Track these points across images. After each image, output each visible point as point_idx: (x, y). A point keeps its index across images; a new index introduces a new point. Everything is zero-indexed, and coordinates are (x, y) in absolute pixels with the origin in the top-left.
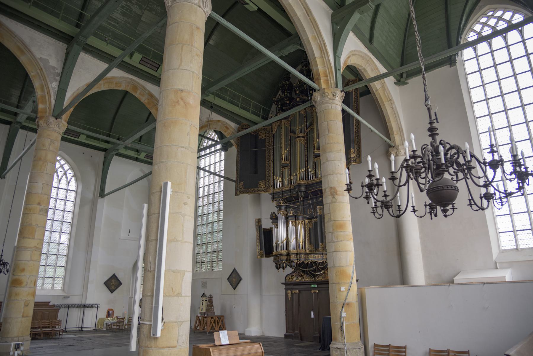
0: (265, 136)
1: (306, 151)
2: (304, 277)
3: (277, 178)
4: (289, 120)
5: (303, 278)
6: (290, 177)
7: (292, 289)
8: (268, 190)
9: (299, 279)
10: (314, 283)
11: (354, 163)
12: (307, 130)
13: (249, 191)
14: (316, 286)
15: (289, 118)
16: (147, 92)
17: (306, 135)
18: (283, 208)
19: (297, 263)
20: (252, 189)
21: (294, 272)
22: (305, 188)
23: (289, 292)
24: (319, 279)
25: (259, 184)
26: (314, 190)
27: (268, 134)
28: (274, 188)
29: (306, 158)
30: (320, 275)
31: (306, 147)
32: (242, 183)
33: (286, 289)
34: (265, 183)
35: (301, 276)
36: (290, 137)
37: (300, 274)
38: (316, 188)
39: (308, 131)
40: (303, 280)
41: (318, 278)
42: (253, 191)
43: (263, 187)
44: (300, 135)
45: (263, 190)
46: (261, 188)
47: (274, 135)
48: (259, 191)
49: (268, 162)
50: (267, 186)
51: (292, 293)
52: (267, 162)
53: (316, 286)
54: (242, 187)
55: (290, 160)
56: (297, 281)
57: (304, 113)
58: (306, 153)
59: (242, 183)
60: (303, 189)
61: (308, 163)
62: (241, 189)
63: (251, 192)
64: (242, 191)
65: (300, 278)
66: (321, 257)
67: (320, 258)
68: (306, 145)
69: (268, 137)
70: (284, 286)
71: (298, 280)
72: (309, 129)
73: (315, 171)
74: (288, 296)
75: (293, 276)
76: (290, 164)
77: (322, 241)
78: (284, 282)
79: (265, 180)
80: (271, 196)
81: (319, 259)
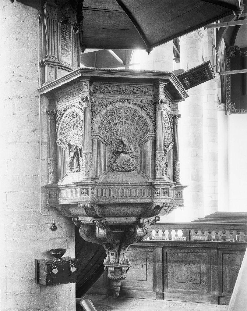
13: (240, 111)
20: (243, 109)
32: (234, 103)
42: (244, 111)
54: (234, 107)
59: (234, 103)
62: (233, 109)
63: (242, 112)
64: (234, 111)
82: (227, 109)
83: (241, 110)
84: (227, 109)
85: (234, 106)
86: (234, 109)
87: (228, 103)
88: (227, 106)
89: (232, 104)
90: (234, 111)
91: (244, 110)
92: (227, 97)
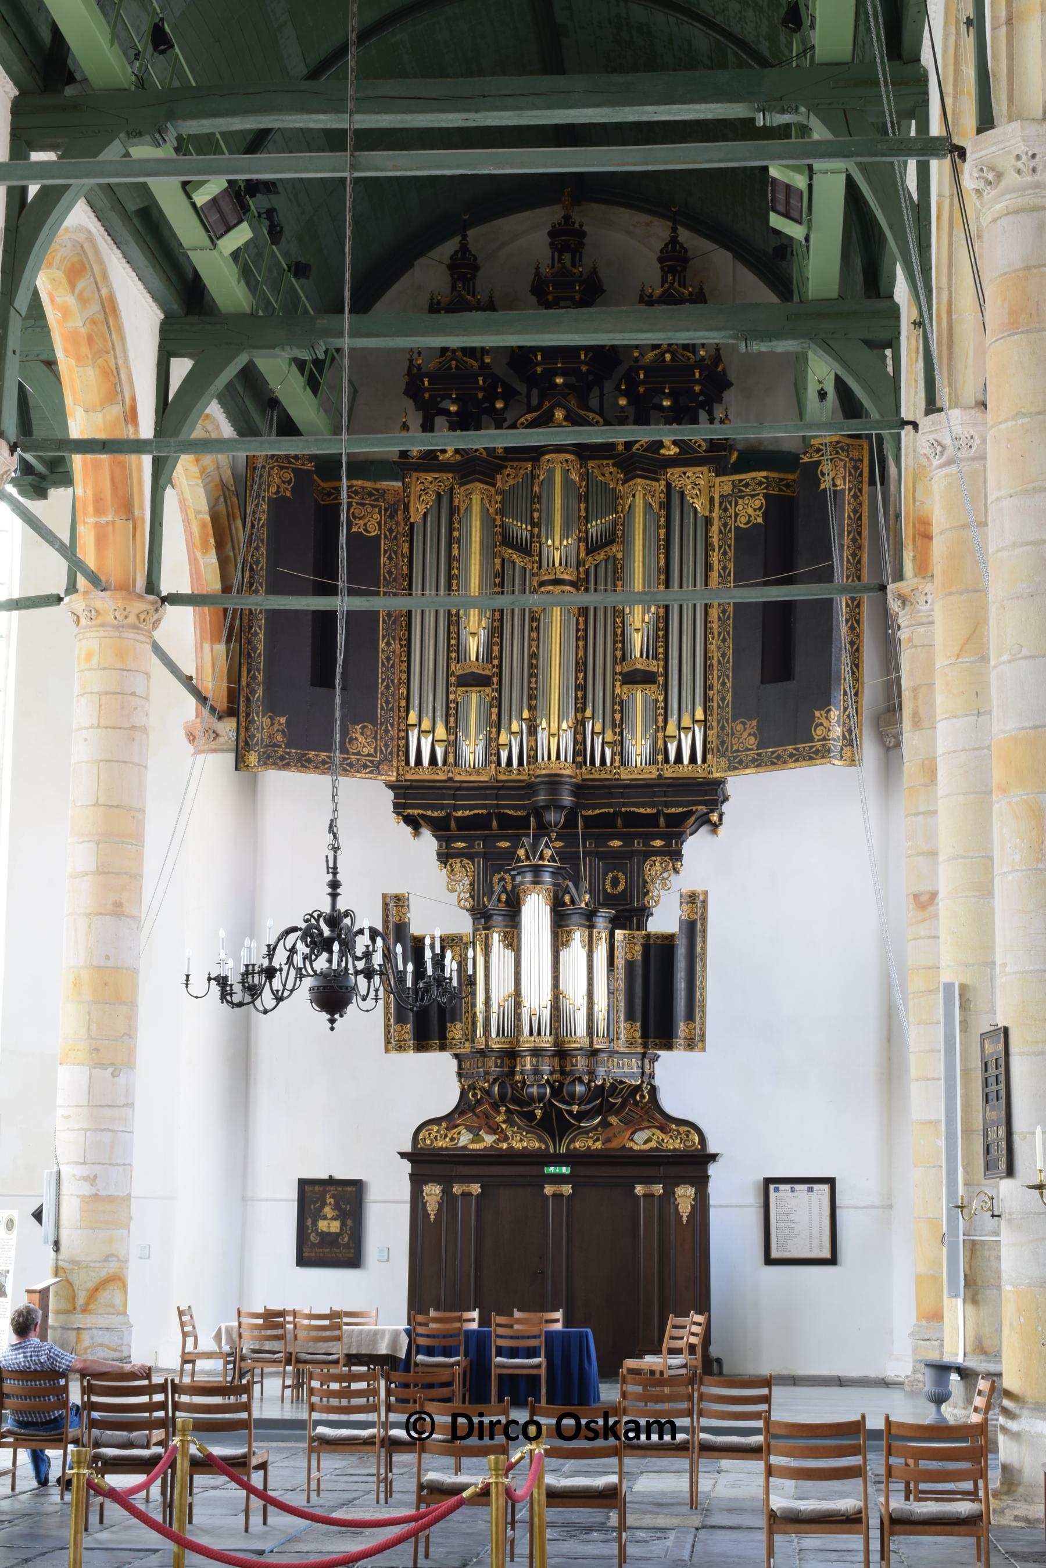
0: (379, 523)
1: (581, 643)
2: (509, 1133)
3: (426, 725)
4: (499, 484)
5: (506, 1139)
6: (494, 735)
7: (446, 1183)
8: (384, 767)
9: (483, 1140)
10: (558, 1160)
11: (836, 762)
12: (590, 558)
13: (309, 761)
14: (565, 1170)
15: (499, 477)
16: (104, 292)
17: (582, 576)
18: (547, 877)
19: (588, 1084)
21: (462, 1113)
22: (574, 793)
23: (433, 1192)
24: (577, 1145)
25: (351, 739)
26: (611, 810)
27: (391, 517)
28: (407, 763)
29: (581, 675)
30: (586, 1132)
31: (582, 626)
32: (283, 720)
33: (417, 1180)
34: (375, 738)
35: (494, 1129)
36: (498, 561)
37: (491, 1123)
38: (624, 805)
39: (590, 563)
40: (505, 1146)
41: (572, 1141)
42: (324, 762)
43: (366, 751)
44: (566, 577)
45: (365, 766)
46: (358, 754)
47: (412, 525)
48: (351, 765)
49: (388, 644)
50: (381, 752)
51: (447, 1192)
52: (382, 645)
53: (565, 1170)
54: (279, 737)
55: (496, 662)
56: (471, 1146)
57: (582, 480)
58: (581, 653)
59: (283, 720)
60: (567, 800)
61: (585, 697)
63: (316, 767)
64: (282, 758)
65: (489, 1139)
66: (638, 1067)
67: (635, 1070)
68: (581, 619)
69: (391, 531)
70: (409, 1164)
71: (481, 1146)
72: (601, 556)
73: (621, 734)
74: (424, 1204)
75: (457, 1126)
76: (495, 680)
77: (690, 1016)
78: (408, 1148)
79: (375, 724)
80: (390, 795)
81: (632, 1076)
82: (247, 743)
83: (311, 754)
84: (247, 743)
85: (283, 731)
86: (280, 746)
87: (248, 715)
88: (247, 729)
89: (272, 724)
90: (282, 758)
91: (324, 760)
92: (248, 685)
